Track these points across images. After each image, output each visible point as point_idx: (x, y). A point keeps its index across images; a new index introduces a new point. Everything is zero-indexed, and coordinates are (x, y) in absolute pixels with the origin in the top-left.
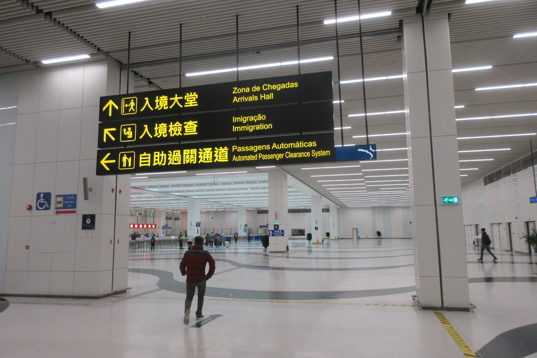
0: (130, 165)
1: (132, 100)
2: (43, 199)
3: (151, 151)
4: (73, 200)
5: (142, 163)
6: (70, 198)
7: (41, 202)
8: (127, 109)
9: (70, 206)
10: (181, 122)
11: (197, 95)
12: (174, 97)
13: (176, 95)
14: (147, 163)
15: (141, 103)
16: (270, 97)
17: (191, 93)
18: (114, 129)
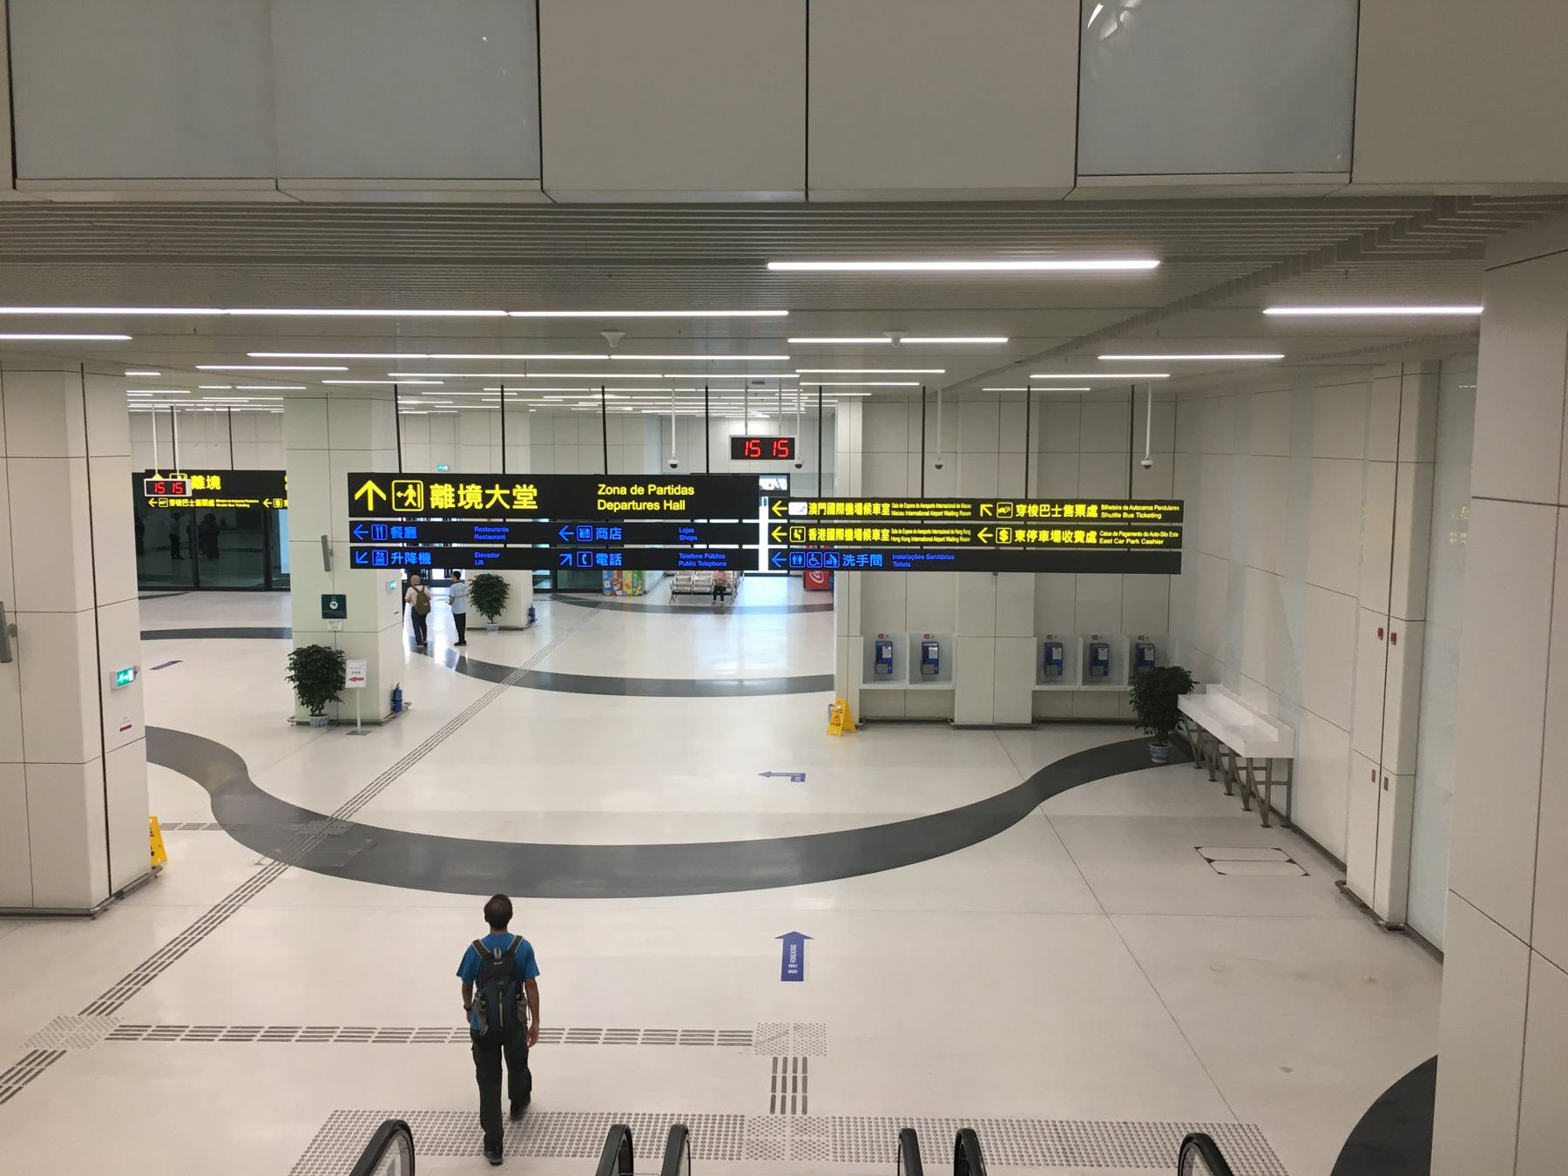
1: (411, 487)
11: (535, 491)
12: (494, 488)
13: (497, 486)
17: (525, 486)
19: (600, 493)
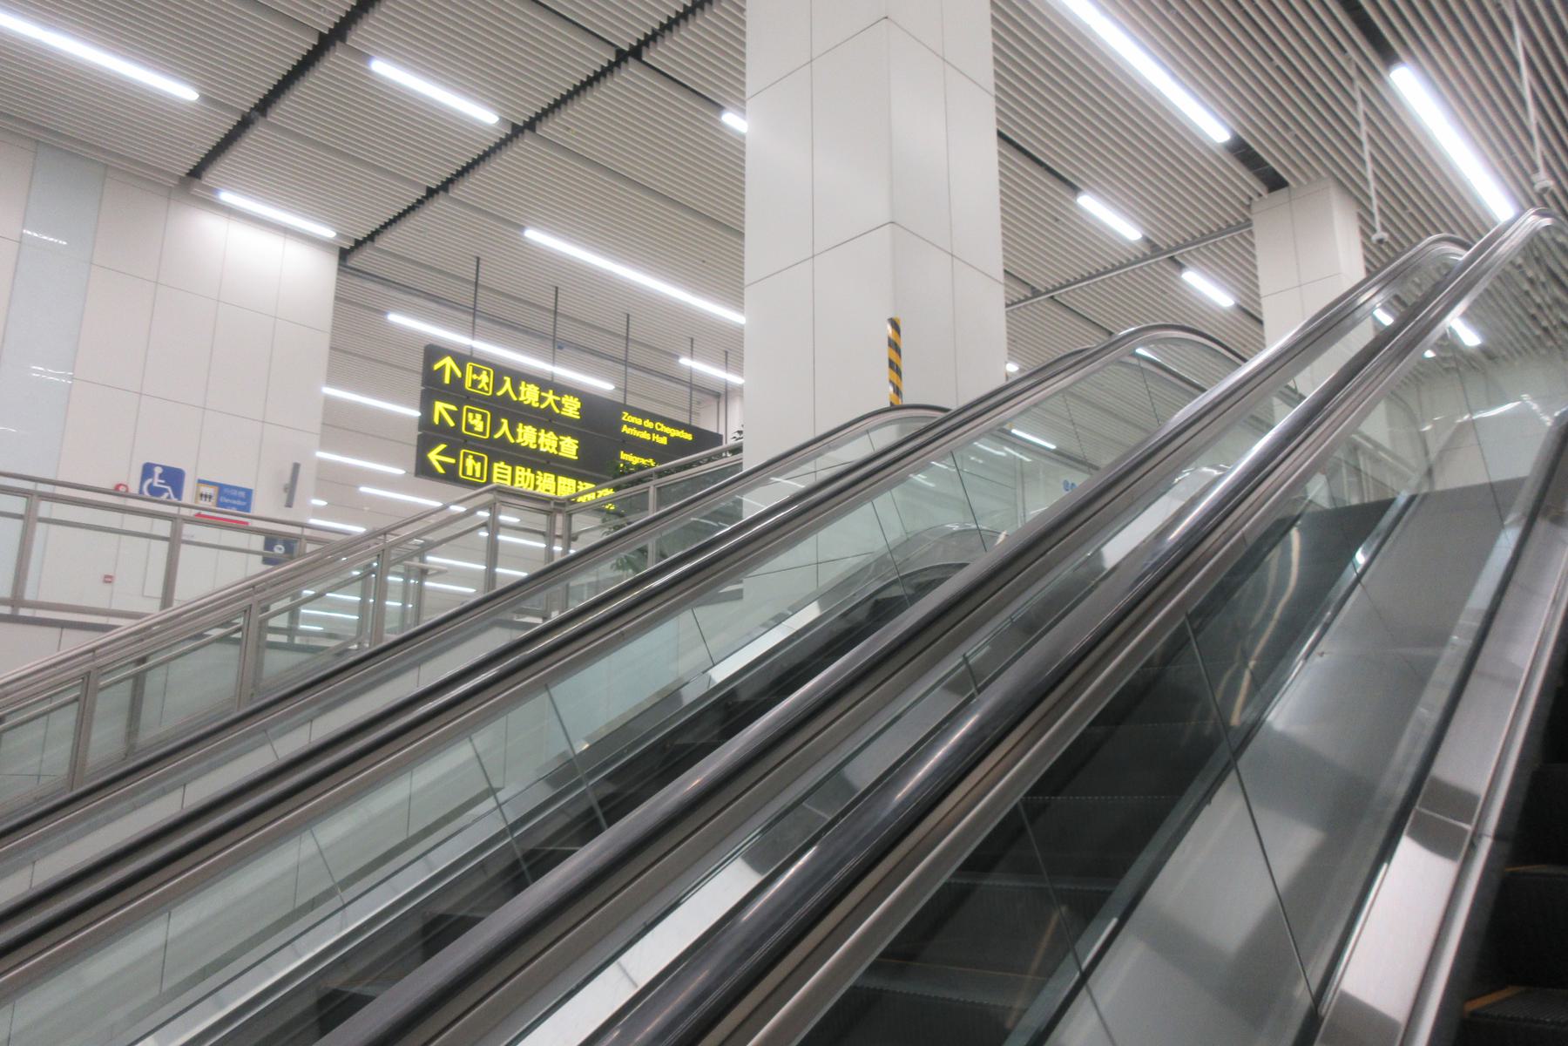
0: (478, 475)
1: (485, 373)
3: (513, 462)
4: (242, 499)
5: (498, 478)
6: (235, 493)
7: (156, 485)
8: (475, 383)
10: (557, 434)
12: (547, 392)
14: (505, 480)
15: (498, 383)
16: (664, 441)
18: (453, 408)
19: (624, 419)
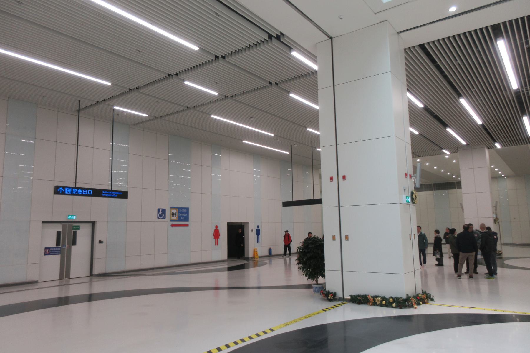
2: (161, 212)
4: (186, 213)
6: (183, 211)
7: (161, 214)
9: (183, 218)
